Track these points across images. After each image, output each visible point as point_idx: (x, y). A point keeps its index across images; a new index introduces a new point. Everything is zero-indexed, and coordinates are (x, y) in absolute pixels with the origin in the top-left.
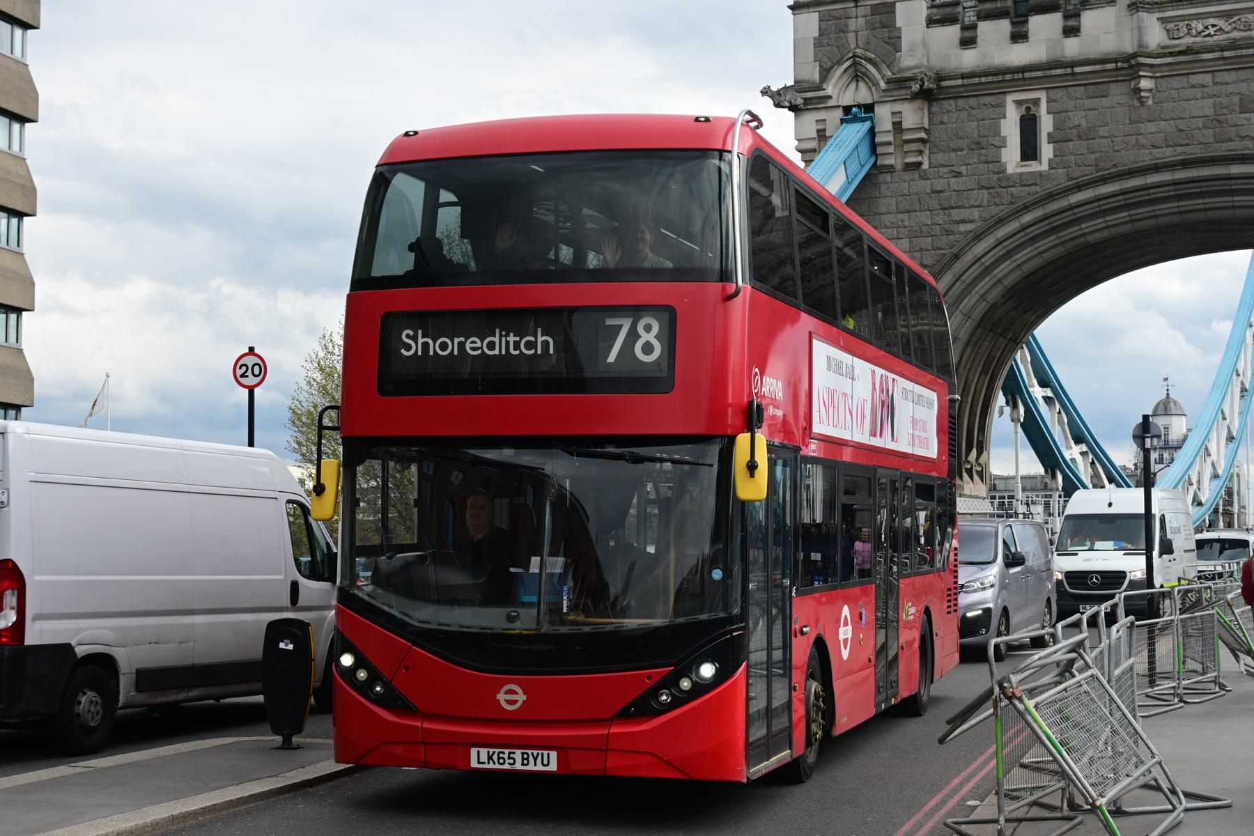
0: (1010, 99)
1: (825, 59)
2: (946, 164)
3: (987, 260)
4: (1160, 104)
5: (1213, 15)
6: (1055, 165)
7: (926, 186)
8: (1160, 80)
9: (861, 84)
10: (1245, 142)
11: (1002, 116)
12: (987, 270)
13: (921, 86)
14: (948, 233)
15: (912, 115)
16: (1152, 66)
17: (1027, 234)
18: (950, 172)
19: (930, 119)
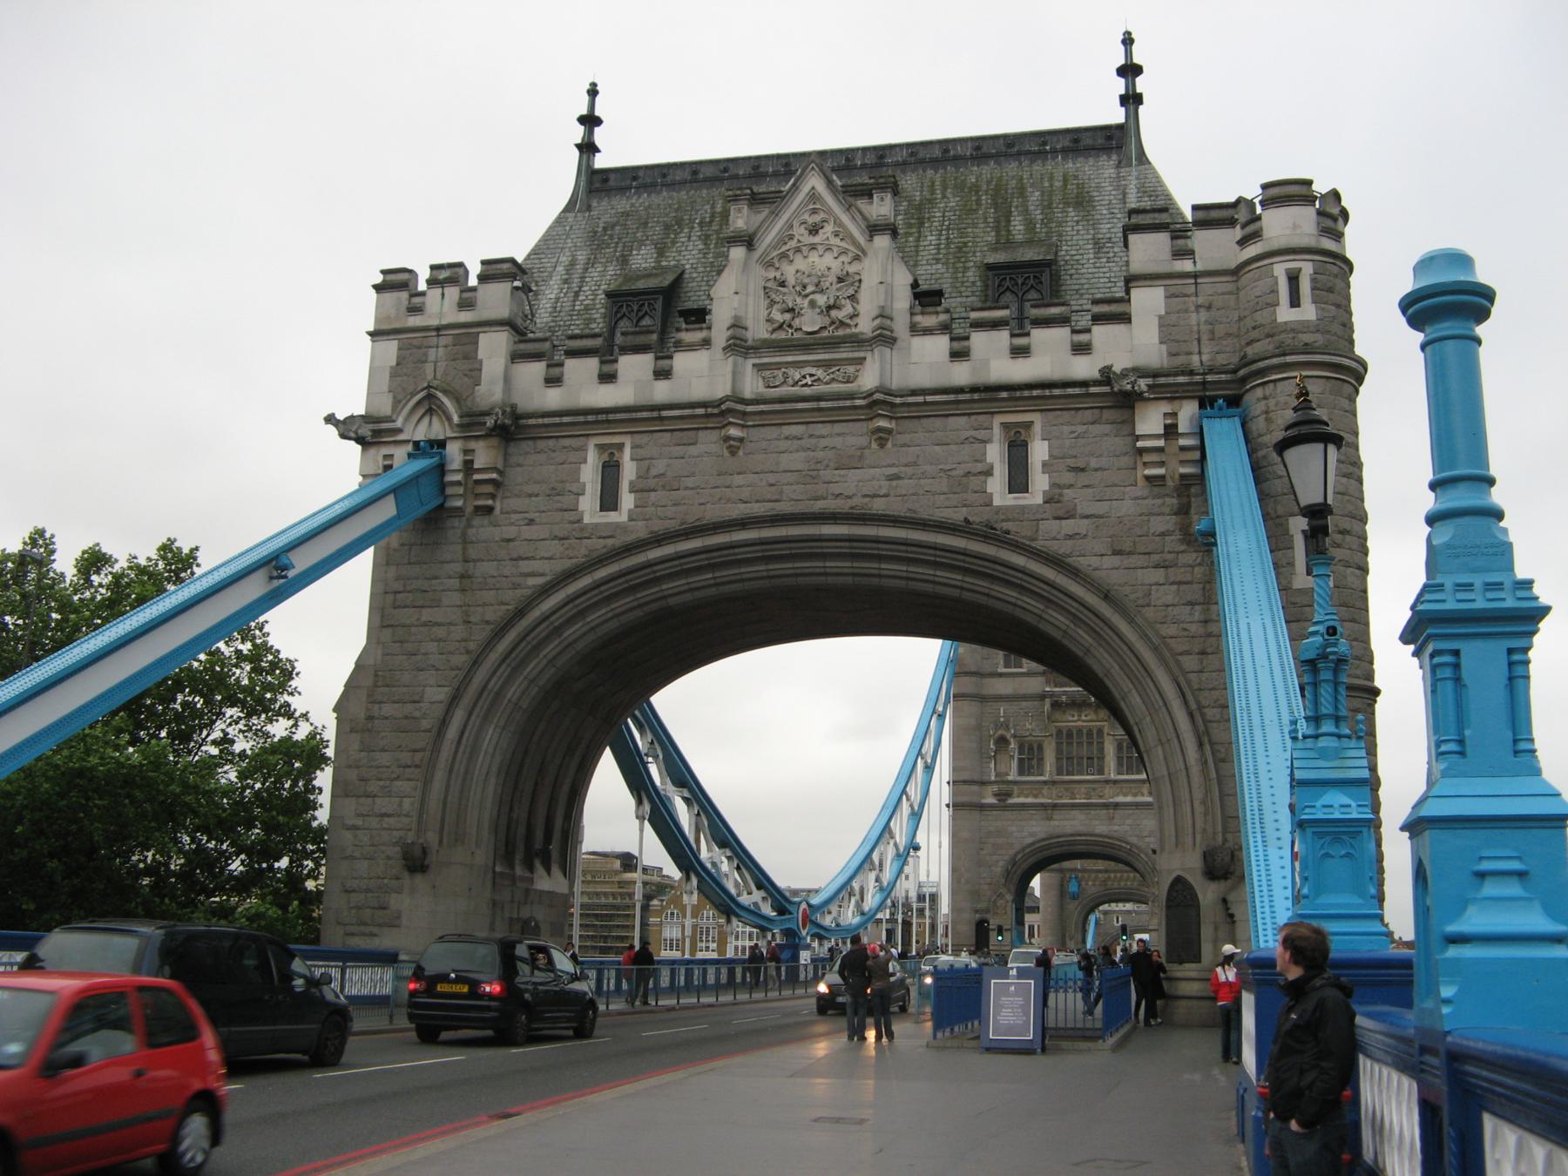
3: (557, 620)
7: (497, 533)
8: (751, 429)
9: (435, 420)
12: (557, 631)
13: (496, 422)
14: (516, 586)
15: (484, 455)
16: (745, 414)
17: (601, 593)
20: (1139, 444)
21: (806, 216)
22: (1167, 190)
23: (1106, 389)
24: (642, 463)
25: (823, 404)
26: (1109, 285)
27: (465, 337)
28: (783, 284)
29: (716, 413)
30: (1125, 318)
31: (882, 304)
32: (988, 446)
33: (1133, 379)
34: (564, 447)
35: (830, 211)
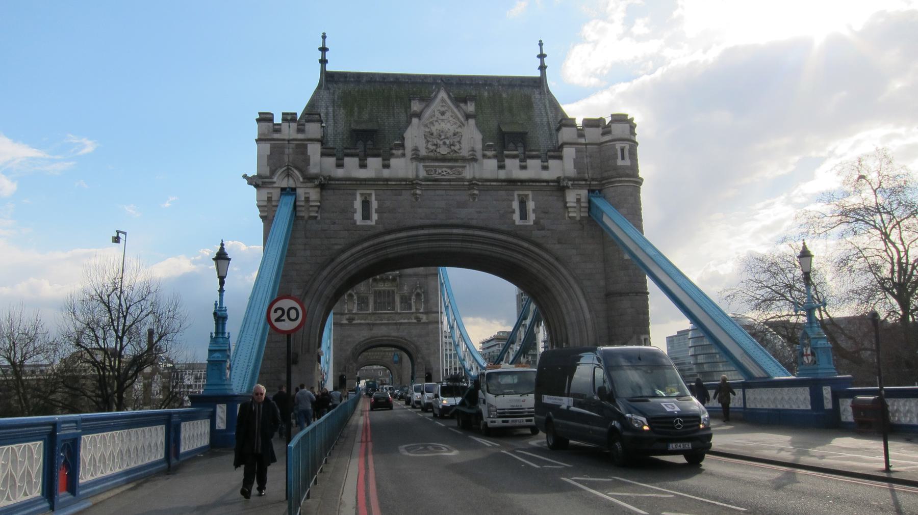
9: (290, 179)
12: (345, 267)
13: (320, 182)
15: (314, 194)
16: (421, 185)
20: (568, 205)
21: (439, 108)
23: (556, 184)
25: (452, 183)
27: (301, 148)
28: (432, 134)
29: (410, 184)
30: (560, 158)
31: (472, 146)
32: (513, 203)
34: (347, 194)
35: (449, 107)
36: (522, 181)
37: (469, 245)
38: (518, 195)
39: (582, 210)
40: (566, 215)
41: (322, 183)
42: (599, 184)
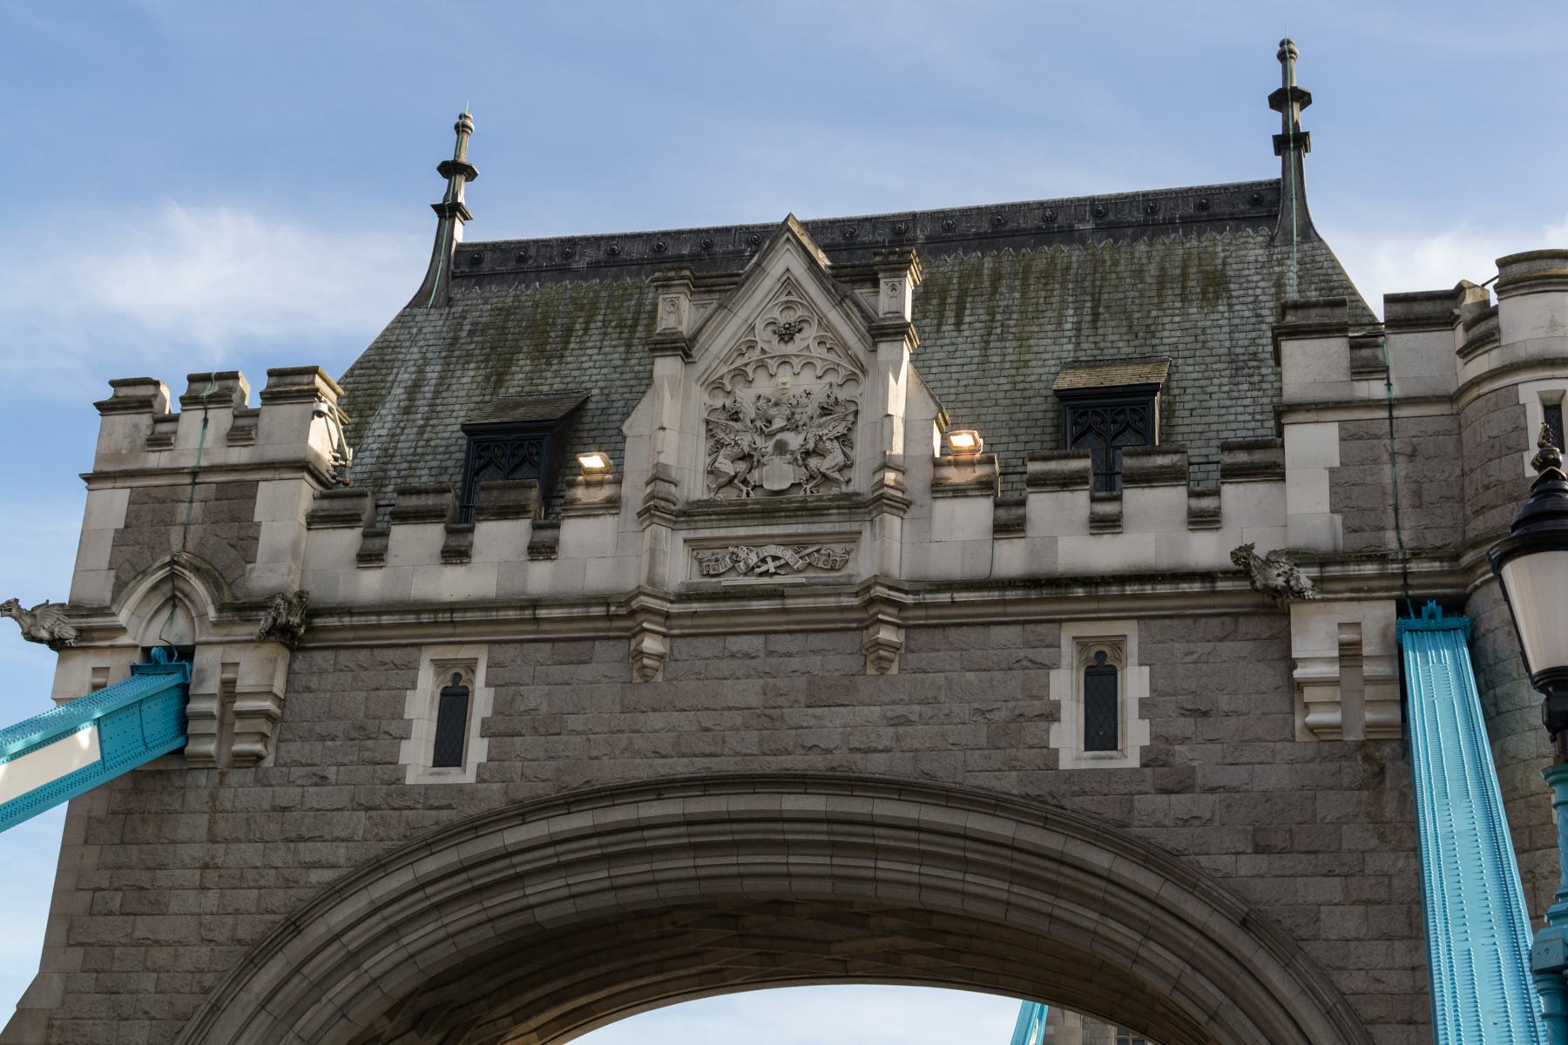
0: (427, 656)
1: (127, 565)
2: (303, 761)
3: (354, 940)
4: (675, 683)
5: (777, 540)
6: (486, 776)
7: (265, 796)
8: (678, 641)
10: (811, 757)
11: (409, 685)
12: (353, 958)
13: (275, 620)
14: (289, 884)
18: (307, 776)
19: (288, 681)
20: (1298, 673)
21: (776, 314)
22: (1347, 279)
23: (1244, 585)
24: (504, 689)
26: (1252, 425)
28: (735, 416)
32: (1053, 674)
33: (1287, 568)
34: (383, 663)
35: (811, 306)
36: (1091, 581)
37: (862, 865)
38: (1076, 639)
39: (1370, 692)
40: (1298, 722)
41: (282, 620)
42: (1451, 573)
